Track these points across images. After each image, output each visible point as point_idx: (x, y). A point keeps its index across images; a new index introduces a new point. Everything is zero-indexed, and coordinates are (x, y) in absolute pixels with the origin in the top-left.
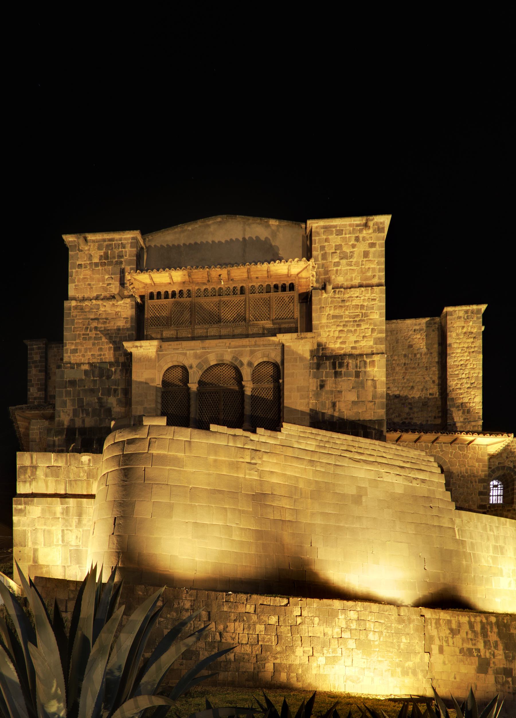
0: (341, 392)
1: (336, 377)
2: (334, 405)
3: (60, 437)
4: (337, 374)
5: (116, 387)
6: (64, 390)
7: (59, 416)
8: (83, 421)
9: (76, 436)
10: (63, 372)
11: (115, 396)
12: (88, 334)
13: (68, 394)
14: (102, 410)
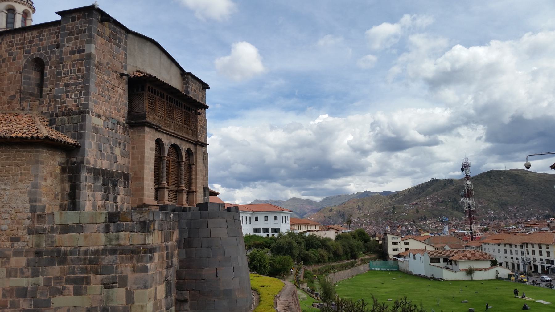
3: (90, 174)
6: (91, 133)
11: (119, 147)
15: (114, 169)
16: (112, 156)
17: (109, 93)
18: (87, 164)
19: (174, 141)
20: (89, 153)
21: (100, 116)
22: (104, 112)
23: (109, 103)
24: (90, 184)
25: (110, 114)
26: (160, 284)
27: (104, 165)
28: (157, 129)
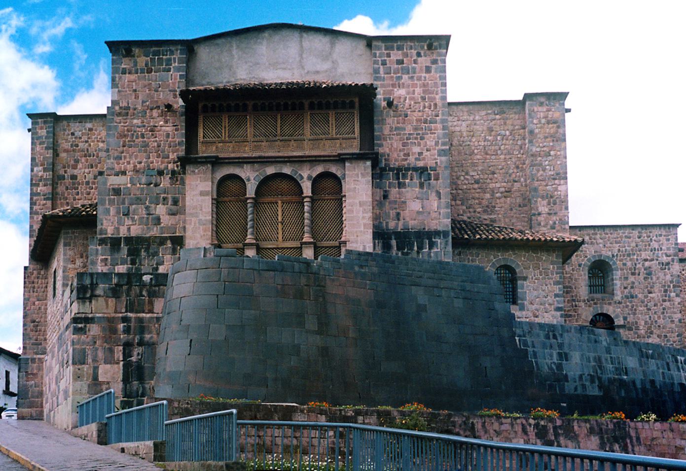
0: (406, 202)
1: (399, 188)
2: (398, 214)
4: (401, 185)
5: (166, 195)
6: (107, 198)
7: (102, 224)
8: (129, 229)
9: (121, 245)
10: (106, 179)
11: (164, 204)
12: (134, 141)
13: (112, 202)
14: (150, 219)
15: (155, 232)
16: (148, 218)
17: (145, 139)
18: (100, 234)
19: (270, 170)
20: (105, 221)
21: (124, 173)
22: (135, 166)
23: (145, 151)
24: (104, 257)
25: (148, 166)
26: (105, 363)
27: (136, 231)
28: (216, 162)
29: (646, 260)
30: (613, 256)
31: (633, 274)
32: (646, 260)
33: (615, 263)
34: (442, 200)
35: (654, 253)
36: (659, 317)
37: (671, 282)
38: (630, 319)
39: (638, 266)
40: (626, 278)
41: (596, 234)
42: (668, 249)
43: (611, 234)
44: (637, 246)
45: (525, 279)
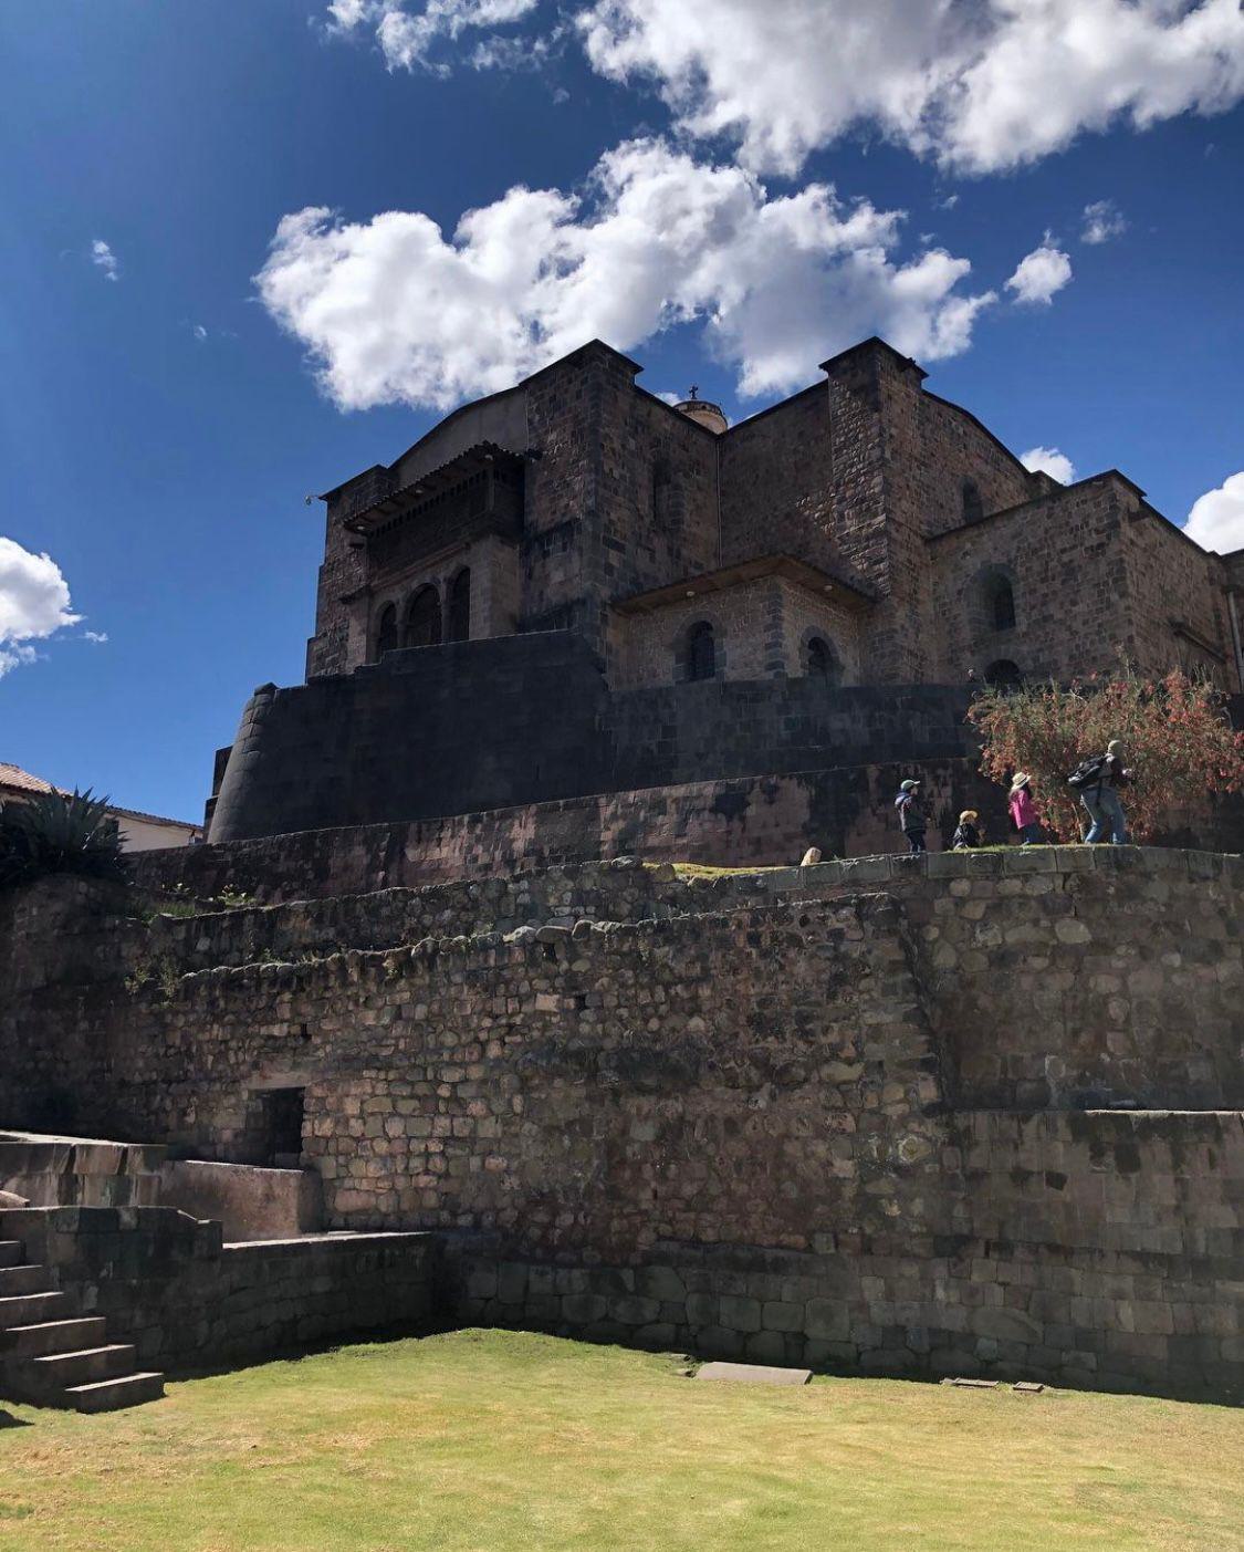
2: (541, 593)
29: (1063, 551)
30: (1010, 561)
31: (1043, 580)
32: (1063, 551)
33: (1013, 572)
34: (585, 558)
35: (1075, 536)
36: (1092, 643)
37: (1109, 574)
38: (1044, 658)
39: (1052, 564)
40: (1033, 591)
41: (982, 534)
42: (1100, 520)
43: (1005, 526)
44: (1046, 531)
45: (724, 634)
